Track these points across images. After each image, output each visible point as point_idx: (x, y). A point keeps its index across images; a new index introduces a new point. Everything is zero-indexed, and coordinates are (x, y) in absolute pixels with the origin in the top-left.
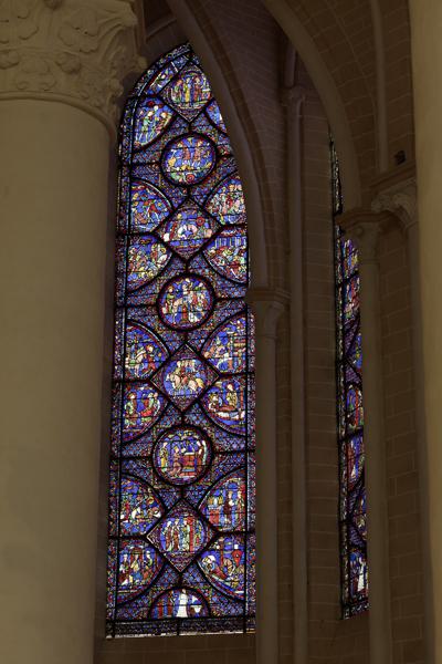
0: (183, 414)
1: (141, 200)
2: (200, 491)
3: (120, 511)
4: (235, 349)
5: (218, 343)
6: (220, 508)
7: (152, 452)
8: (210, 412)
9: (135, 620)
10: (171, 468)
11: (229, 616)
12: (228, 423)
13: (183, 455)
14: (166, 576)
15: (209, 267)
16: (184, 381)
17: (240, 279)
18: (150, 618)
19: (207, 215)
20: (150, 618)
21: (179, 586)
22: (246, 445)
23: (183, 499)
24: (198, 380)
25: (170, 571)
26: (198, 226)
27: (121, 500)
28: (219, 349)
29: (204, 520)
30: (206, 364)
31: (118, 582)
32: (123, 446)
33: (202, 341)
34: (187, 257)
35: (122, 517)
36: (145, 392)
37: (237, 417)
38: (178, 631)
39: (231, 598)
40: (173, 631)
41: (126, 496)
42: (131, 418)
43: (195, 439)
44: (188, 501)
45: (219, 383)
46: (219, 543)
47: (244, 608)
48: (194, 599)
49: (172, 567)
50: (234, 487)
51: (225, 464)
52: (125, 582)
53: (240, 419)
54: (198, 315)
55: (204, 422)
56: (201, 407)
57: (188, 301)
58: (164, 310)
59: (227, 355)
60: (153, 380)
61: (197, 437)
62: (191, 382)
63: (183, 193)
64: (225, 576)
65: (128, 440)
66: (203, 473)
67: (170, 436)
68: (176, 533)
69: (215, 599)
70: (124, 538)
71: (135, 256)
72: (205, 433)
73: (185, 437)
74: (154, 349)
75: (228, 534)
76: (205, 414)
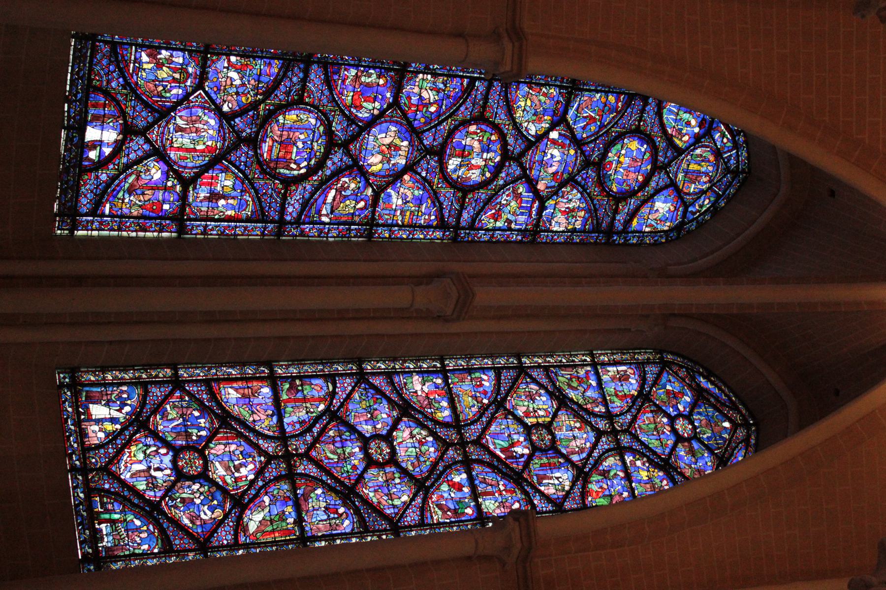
0: (345, 145)
1: (606, 105)
2: (245, 163)
3: (241, 56)
4: (403, 213)
5: (416, 193)
6: (219, 188)
7: (307, 104)
8: (339, 180)
9: (91, 70)
10: (283, 127)
11: (77, 194)
12: (320, 200)
13: (295, 144)
14: (144, 114)
15: (506, 184)
16: (383, 149)
17: (480, 221)
18: (90, 88)
19: (562, 184)
20: (90, 88)
21: (128, 131)
22: (290, 223)
23: (240, 140)
24: (380, 166)
25: (150, 119)
26: (555, 174)
27: (254, 58)
28: (409, 194)
29: (205, 169)
30: (395, 177)
31: (149, 47)
32: (324, 65)
33: (424, 174)
34: (524, 160)
35: (233, 59)
36: (384, 97)
37: (324, 212)
38: (68, 128)
39: (103, 197)
40: (69, 121)
41: (259, 65)
42: (357, 77)
43: (310, 160)
44: (235, 147)
45: (369, 192)
46: (174, 186)
47: (86, 215)
48: (107, 151)
50: (242, 205)
51: (271, 196)
52: (145, 58)
53: (321, 215)
54: (455, 170)
55: (328, 172)
56: (349, 168)
57: (474, 157)
58: (473, 128)
59: (400, 202)
60: (395, 110)
61: (313, 162)
62: (379, 158)
63: (595, 157)
64: (131, 191)
65: (330, 69)
66: (268, 169)
67: (322, 129)
68: (197, 131)
70: (205, 59)
71: (545, 95)
72: (316, 173)
73: (316, 147)
74: (432, 113)
75: (184, 197)
76: (337, 173)
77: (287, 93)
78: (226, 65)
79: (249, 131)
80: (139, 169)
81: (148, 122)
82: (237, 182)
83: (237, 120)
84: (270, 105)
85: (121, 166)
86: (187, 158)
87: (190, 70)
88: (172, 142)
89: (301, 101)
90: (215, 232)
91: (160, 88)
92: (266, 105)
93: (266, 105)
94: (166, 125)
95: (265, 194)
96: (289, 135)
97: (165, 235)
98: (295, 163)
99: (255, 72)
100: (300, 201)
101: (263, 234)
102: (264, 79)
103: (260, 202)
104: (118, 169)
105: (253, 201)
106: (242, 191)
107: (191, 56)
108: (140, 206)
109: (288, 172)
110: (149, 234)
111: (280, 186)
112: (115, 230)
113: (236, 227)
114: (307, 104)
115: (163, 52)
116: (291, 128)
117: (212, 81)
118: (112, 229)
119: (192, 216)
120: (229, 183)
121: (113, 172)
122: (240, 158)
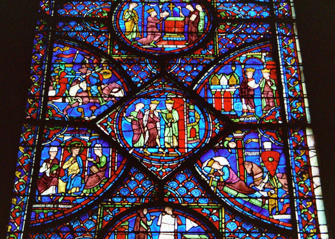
2: (193, 65)
3: (48, 85)
7: (110, 14)
10: (143, 32)
13: (163, 20)
14: (132, 185)
21: (159, 202)
25: (140, 177)
27: (50, 71)
35: (52, 93)
44: (174, 81)
46: (235, 140)
48: (190, 224)
49: (144, 171)
51: (236, 34)
52: (51, 191)
64: (250, 191)
68: (152, 121)
69: (232, 226)
70: (53, 123)
75: (250, 128)
77: (97, 34)
78: (60, 100)
79: (149, 67)
80: (215, 183)
81: (144, 179)
82: (221, 71)
83: (137, 80)
84: (112, 50)
85: (213, 206)
86: (193, 128)
87: (67, 138)
88: (173, 148)
89: (107, 21)
90: (297, 88)
91: (94, 169)
92: (114, 54)
93: (114, 54)
94: (148, 157)
95: (234, 40)
96: (152, 26)
97: (310, 142)
98: (190, 16)
99: (69, 70)
100: (240, 5)
101: (291, 37)
102: (78, 58)
103: (246, 44)
104: (218, 210)
105: (246, 52)
106: (234, 65)
107: (49, 139)
108: (271, 177)
109: (202, 23)
110: (314, 161)
111: (222, 27)
112: (314, 204)
113: (285, 65)
114: (110, 14)
115: (42, 170)
116: (143, 26)
117: (83, 113)
118: (314, 208)
119: (278, 115)
120: (224, 80)
121: (223, 213)
122: (187, 72)
